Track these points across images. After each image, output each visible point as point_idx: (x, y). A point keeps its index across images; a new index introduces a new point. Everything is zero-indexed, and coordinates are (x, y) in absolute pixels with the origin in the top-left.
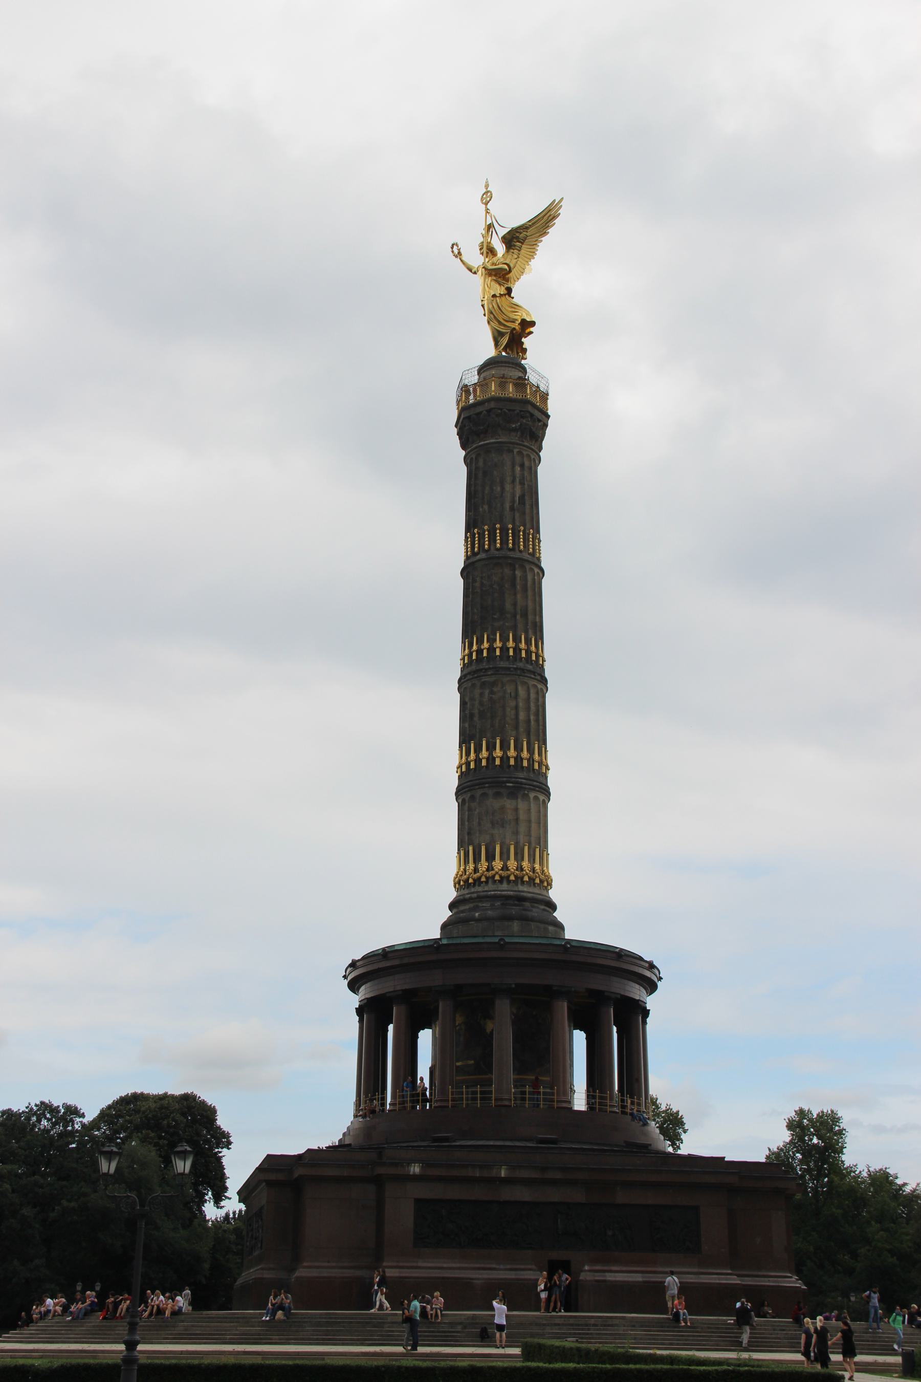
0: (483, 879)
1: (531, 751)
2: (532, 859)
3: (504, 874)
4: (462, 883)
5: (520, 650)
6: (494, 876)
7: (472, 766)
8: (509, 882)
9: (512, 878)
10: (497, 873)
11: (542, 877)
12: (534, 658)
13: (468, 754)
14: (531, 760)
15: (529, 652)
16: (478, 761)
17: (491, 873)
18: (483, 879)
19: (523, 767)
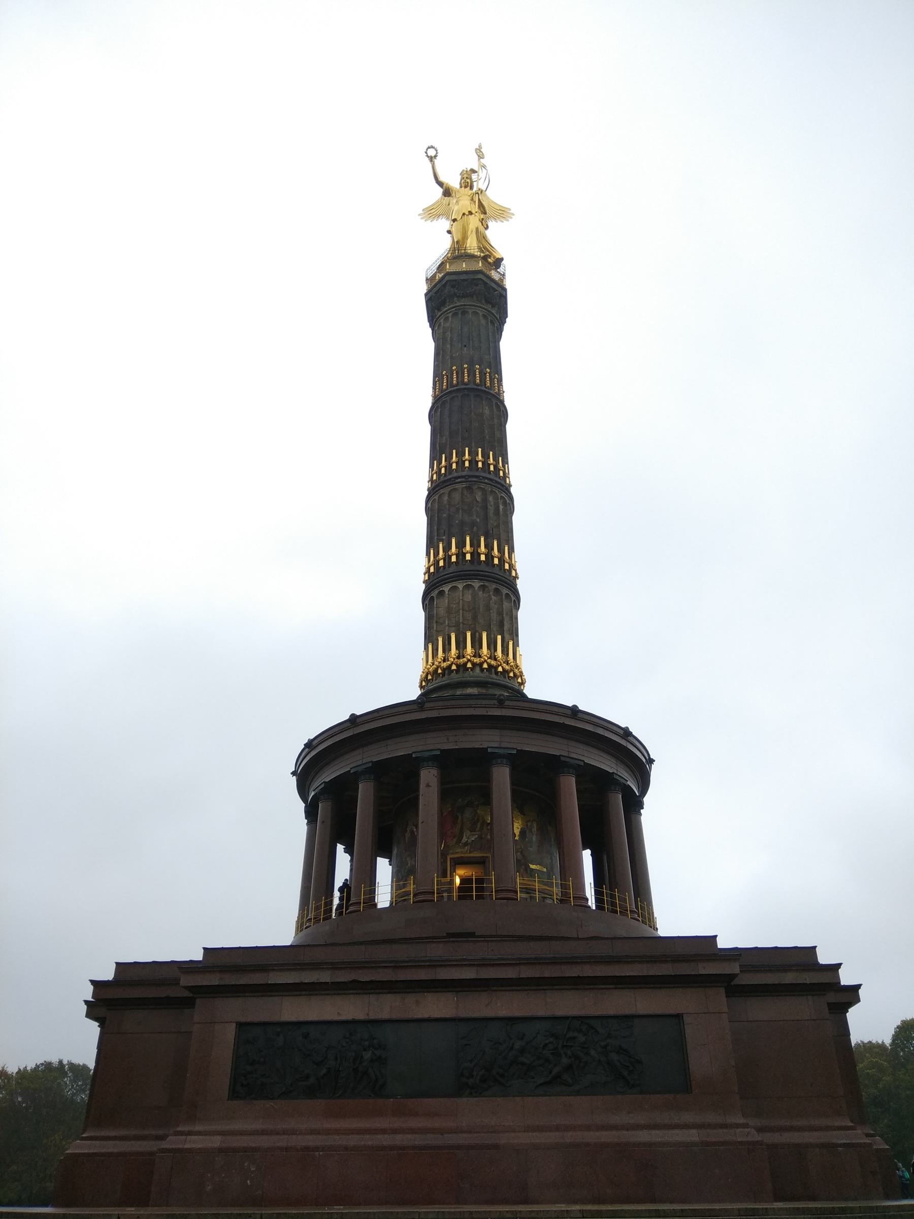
0: (454, 667)
1: (501, 550)
2: (505, 651)
3: (477, 660)
4: (430, 677)
5: (489, 465)
6: (466, 664)
7: (441, 563)
8: (482, 670)
9: (485, 666)
10: (469, 660)
11: (516, 671)
12: (501, 474)
13: (436, 554)
14: (502, 560)
15: (495, 467)
16: (447, 558)
17: (462, 661)
18: (454, 667)
19: (494, 565)
